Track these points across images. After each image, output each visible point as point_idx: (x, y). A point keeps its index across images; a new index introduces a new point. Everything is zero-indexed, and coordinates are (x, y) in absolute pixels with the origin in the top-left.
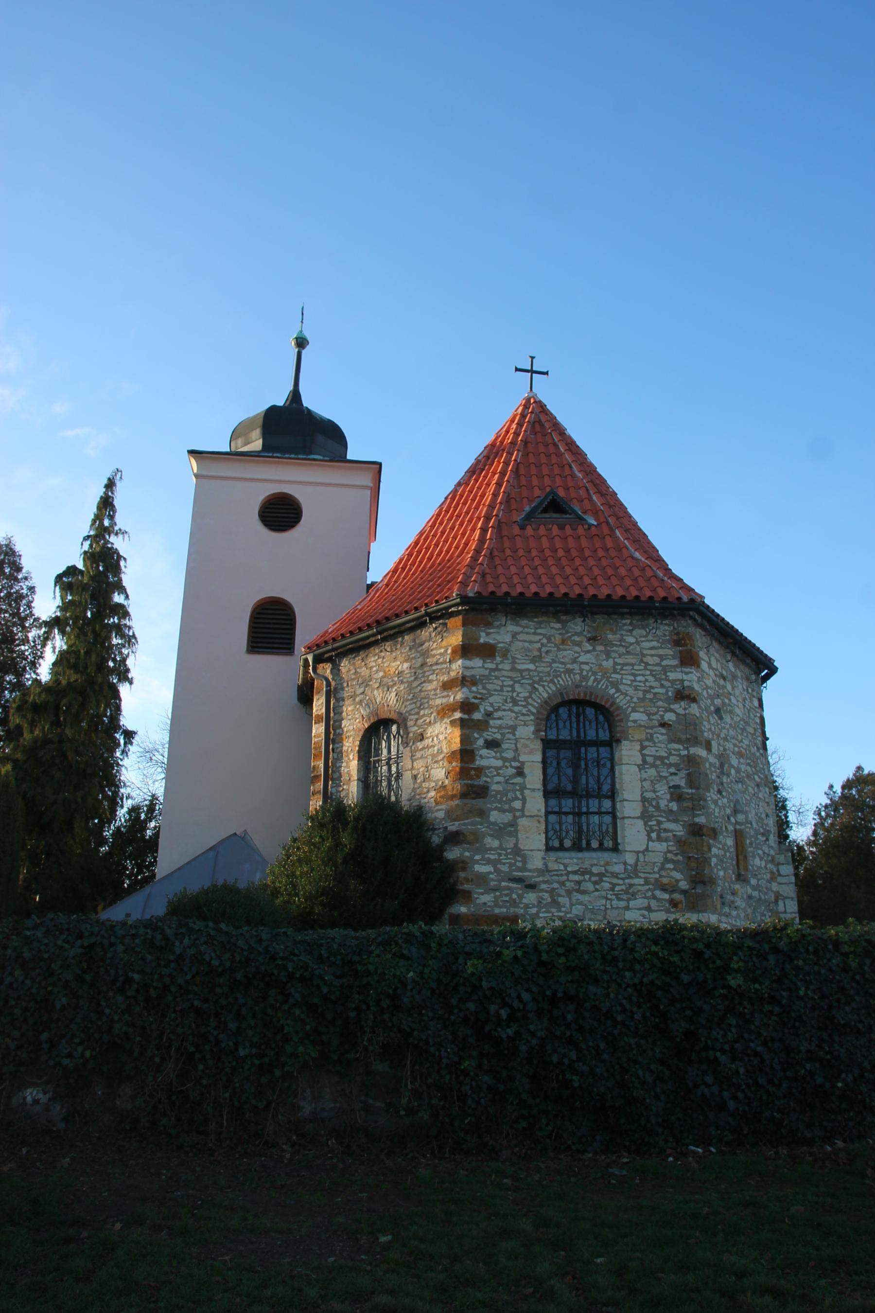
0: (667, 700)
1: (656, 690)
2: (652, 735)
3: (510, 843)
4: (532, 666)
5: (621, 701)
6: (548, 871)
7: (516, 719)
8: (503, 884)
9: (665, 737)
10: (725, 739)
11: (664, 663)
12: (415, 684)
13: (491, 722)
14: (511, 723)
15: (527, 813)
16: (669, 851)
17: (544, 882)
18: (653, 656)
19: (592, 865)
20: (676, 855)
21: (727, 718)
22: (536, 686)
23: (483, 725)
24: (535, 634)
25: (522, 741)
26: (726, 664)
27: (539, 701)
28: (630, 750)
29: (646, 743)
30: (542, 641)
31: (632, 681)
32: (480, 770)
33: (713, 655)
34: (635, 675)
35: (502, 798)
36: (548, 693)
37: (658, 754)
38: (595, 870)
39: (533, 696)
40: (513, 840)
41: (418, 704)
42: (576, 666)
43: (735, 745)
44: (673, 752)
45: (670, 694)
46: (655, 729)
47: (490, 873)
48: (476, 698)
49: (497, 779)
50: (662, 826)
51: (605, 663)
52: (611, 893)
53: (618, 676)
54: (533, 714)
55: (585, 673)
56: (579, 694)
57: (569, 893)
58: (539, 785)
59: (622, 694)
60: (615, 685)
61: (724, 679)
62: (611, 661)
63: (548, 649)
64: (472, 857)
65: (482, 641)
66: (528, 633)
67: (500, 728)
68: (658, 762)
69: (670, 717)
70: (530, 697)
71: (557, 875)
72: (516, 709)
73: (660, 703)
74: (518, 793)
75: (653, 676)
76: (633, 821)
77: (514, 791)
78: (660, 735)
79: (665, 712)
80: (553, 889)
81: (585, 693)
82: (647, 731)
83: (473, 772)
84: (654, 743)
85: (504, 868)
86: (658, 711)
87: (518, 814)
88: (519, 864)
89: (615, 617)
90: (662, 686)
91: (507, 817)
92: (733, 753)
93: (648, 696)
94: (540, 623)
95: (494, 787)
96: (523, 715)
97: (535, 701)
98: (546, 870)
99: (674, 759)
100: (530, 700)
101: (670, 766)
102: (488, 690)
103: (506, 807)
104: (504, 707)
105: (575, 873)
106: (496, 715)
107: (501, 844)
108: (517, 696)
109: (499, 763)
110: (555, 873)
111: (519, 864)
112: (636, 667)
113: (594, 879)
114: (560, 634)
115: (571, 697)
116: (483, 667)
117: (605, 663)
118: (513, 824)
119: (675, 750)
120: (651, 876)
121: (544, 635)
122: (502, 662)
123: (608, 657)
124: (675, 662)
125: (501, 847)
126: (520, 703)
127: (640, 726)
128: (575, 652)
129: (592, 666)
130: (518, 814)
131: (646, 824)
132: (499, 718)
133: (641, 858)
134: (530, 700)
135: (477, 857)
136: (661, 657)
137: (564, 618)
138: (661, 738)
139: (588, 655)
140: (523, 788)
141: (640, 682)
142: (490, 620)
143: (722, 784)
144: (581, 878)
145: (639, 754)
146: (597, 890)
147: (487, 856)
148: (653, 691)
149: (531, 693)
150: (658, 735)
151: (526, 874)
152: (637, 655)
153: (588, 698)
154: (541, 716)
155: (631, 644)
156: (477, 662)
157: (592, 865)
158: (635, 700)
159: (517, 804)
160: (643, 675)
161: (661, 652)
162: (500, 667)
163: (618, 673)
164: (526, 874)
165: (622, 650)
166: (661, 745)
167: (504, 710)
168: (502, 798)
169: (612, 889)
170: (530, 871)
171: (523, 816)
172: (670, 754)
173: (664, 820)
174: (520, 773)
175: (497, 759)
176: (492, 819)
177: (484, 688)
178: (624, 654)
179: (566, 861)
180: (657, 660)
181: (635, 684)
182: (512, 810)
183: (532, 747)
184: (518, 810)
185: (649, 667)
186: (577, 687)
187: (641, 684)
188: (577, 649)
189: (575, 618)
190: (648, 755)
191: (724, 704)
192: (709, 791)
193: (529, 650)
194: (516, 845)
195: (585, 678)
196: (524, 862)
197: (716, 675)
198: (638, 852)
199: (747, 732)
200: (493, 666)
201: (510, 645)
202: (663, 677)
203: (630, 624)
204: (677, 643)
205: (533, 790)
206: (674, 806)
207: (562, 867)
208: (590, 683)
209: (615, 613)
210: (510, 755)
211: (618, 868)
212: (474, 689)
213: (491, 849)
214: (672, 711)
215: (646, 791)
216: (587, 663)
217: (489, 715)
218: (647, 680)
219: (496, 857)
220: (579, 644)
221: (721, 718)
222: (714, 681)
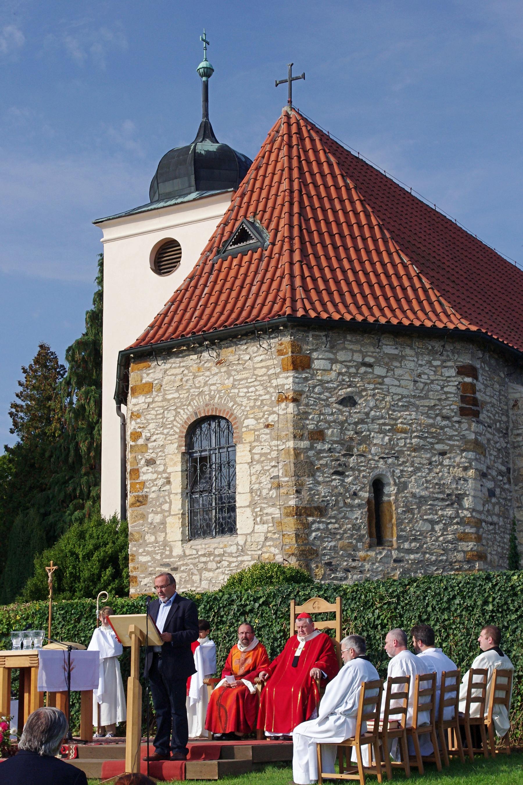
0: (272, 405)
1: (264, 397)
2: (258, 436)
3: (161, 539)
5: (237, 412)
6: (185, 555)
7: (165, 439)
8: (157, 569)
9: (268, 436)
10: (362, 421)
11: (271, 372)
13: (150, 445)
14: (161, 443)
15: (172, 513)
16: (268, 532)
17: (183, 565)
18: (262, 367)
19: (215, 549)
20: (275, 533)
22: (179, 410)
24: (179, 367)
25: (169, 456)
26: (378, 350)
27: (181, 422)
28: (243, 451)
30: (184, 372)
31: (246, 393)
32: (144, 483)
33: (345, 348)
34: (248, 387)
35: (156, 503)
36: (187, 414)
37: (263, 451)
38: (216, 552)
39: (177, 418)
40: (163, 535)
42: (206, 389)
43: (385, 424)
44: (274, 448)
45: (273, 398)
46: (262, 431)
47: (149, 562)
48: (140, 428)
49: (154, 489)
50: (265, 511)
51: (226, 382)
52: (228, 569)
53: (236, 391)
54: (177, 433)
56: (208, 411)
57: (200, 571)
59: (239, 405)
60: (233, 399)
61: (370, 365)
62: (231, 378)
63: (188, 378)
64: (137, 551)
65: (144, 381)
66: (175, 368)
68: (263, 458)
69: (273, 418)
70: (175, 420)
71: (192, 559)
72: (165, 431)
74: (167, 498)
75: (262, 385)
76: (244, 509)
77: (164, 497)
78: (265, 435)
79: (269, 415)
80: (190, 570)
81: (212, 410)
82: (256, 433)
83: (138, 486)
84: (261, 442)
85: (158, 557)
86: (264, 415)
87: (166, 514)
88: (167, 553)
90: (268, 393)
91: (158, 518)
92: (380, 432)
93: (258, 403)
95: (152, 496)
96: (171, 435)
97: (178, 423)
98: (184, 555)
99: (274, 454)
100: (175, 423)
101: (272, 459)
104: (157, 432)
105: (204, 555)
106: (153, 438)
107: (156, 538)
108: (166, 421)
109: (155, 476)
110: (190, 557)
111: (167, 553)
112: (249, 381)
113: (218, 559)
114: (196, 363)
115: (203, 415)
116: (145, 402)
117: (226, 382)
118: (163, 523)
119: (275, 446)
120: (256, 553)
121: (187, 368)
122: (157, 395)
123: (229, 375)
124: (278, 370)
125: (156, 542)
126: (168, 426)
127: (251, 430)
128: (207, 377)
129: (217, 385)
130: (166, 514)
131: (253, 511)
132: (155, 441)
133: (249, 540)
134: (175, 423)
135: (141, 551)
136: (268, 368)
139: (216, 378)
140: (170, 493)
141: (252, 392)
144: (208, 559)
145: (249, 453)
146: (218, 568)
147: (146, 549)
148: (261, 398)
149: (175, 416)
150: (263, 436)
151: (172, 560)
152: (250, 369)
153: (214, 414)
154: (182, 434)
155: (246, 361)
157: (215, 549)
158: (248, 409)
160: (254, 386)
161: (270, 363)
162: (156, 399)
163: (236, 388)
164: (172, 560)
165: (241, 367)
167: (157, 434)
168: (156, 503)
169: (229, 566)
170: (174, 557)
171: (170, 515)
172: (272, 450)
173: (265, 506)
174: (169, 482)
175: (153, 473)
176: (149, 520)
177: (145, 419)
178: (241, 371)
179: (198, 547)
180: (264, 370)
181: (248, 395)
182: (163, 511)
183: (176, 460)
184: (167, 511)
185: (258, 378)
186: (207, 405)
187: (253, 394)
188: (208, 373)
190: (256, 454)
192: (313, 475)
193: (174, 382)
194: (165, 538)
195: (212, 398)
196: (171, 551)
197: (348, 367)
198: (246, 535)
199: (417, 407)
200: (150, 400)
201: (162, 381)
202: (269, 384)
204: (280, 352)
205: (176, 494)
206: (273, 493)
207: (194, 552)
210: (161, 468)
211: (233, 549)
212: (138, 420)
213: (150, 543)
214: (274, 413)
215: (254, 484)
216: (214, 384)
217: (148, 439)
218: (256, 390)
219: (153, 549)
220: (209, 369)
221: (354, 404)
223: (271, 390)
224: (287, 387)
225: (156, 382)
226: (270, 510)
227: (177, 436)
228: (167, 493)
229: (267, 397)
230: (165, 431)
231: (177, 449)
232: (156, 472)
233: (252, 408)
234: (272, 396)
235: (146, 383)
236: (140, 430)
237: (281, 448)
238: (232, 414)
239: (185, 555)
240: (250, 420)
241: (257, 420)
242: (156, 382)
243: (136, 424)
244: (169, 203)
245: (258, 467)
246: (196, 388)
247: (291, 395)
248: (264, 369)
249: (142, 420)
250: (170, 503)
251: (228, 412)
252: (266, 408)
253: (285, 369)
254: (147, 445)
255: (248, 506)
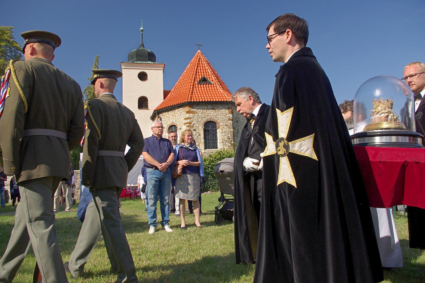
1: (225, 119)
4: (201, 115)
5: (218, 121)
11: (226, 113)
12: (179, 118)
13: (194, 126)
14: (198, 126)
17: (205, 155)
18: (224, 112)
21: (239, 122)
23: (193, 127)
29: (223, 129)
34: (221, 116)
37: (225, 131)
39: (202, 120)
41: (180, 122)
42: (209, 114)
43: (240, 127)
48: (191, 121)
49: (196, 136)
53: (218, 116)
55: (211, 116)
58: (203, 137)
60: (217, 118)
61: (238, 115)
62: (216, 113)
65: (192, 110)
67: (195, 127)
69: (227, 123)
72: (199, 123)
73: (225, 121)
78: (225, 127)
79: (226, 123)
81: (212, 120)
84: (224, 128)
86: (225, 122)
89: (217, 104)
92: (240, 129)
94: (203, 106)
99: (228, 132)
102: (193, 120)
103: (197, 141)
106: (195, 124)
117: (215, 114)
132: (196, 125)
137: (207, 105)
138: (225, 127)
139: (212, 112)
140: (200, 138)
142: (193, 106)
143: (237, 135)
156: (191, 115)
159: (200, 141)
166: (226, 129)
171: (201, 143)
174: (200, 135)
177: (193, 119)
182: (199, 142)
186: (210, 118)
189: (209, 105)
191: (238, 120)
195: (212, 117)
197: (237, 114)
200: (194, 115)
203: (220, 106)
205: (202, 138)
207: (208, 152)
208: (212, 117)
209: (217, 104)
210: (198, 132)
212: (190, 119)
214: (227, 122)
216: (211, 114)
221: (237, 123)
222: (236, 116)
223: (227, 117)
224: (230, 117)
225: (195, 111)
226: (227, 144)
227: (202, 125)
228: (199, 138)
229: (226, 118)
230: (199, 123)
231: (202, 127)
232: (196, 132)
233: (222, 120)
234: (227, 119)
235: (192, 111)
236: (191, 122)
237: (230, 130)
238: (217, 121)
239: (205, 153)
240: (221, 123)
241: (223, 123)
242: (195, 111)
243: (190, 120)
244: (143, 63)
245: (224, 134)
246: (207, 114)
247: (232, 119)
248: (225, 112)
249: (192, 120)
250: (201, 140)
251: (216, 121)
252: (225, 121)
253: (230, 113)
254: (193, 126)
255: (222, 142)
